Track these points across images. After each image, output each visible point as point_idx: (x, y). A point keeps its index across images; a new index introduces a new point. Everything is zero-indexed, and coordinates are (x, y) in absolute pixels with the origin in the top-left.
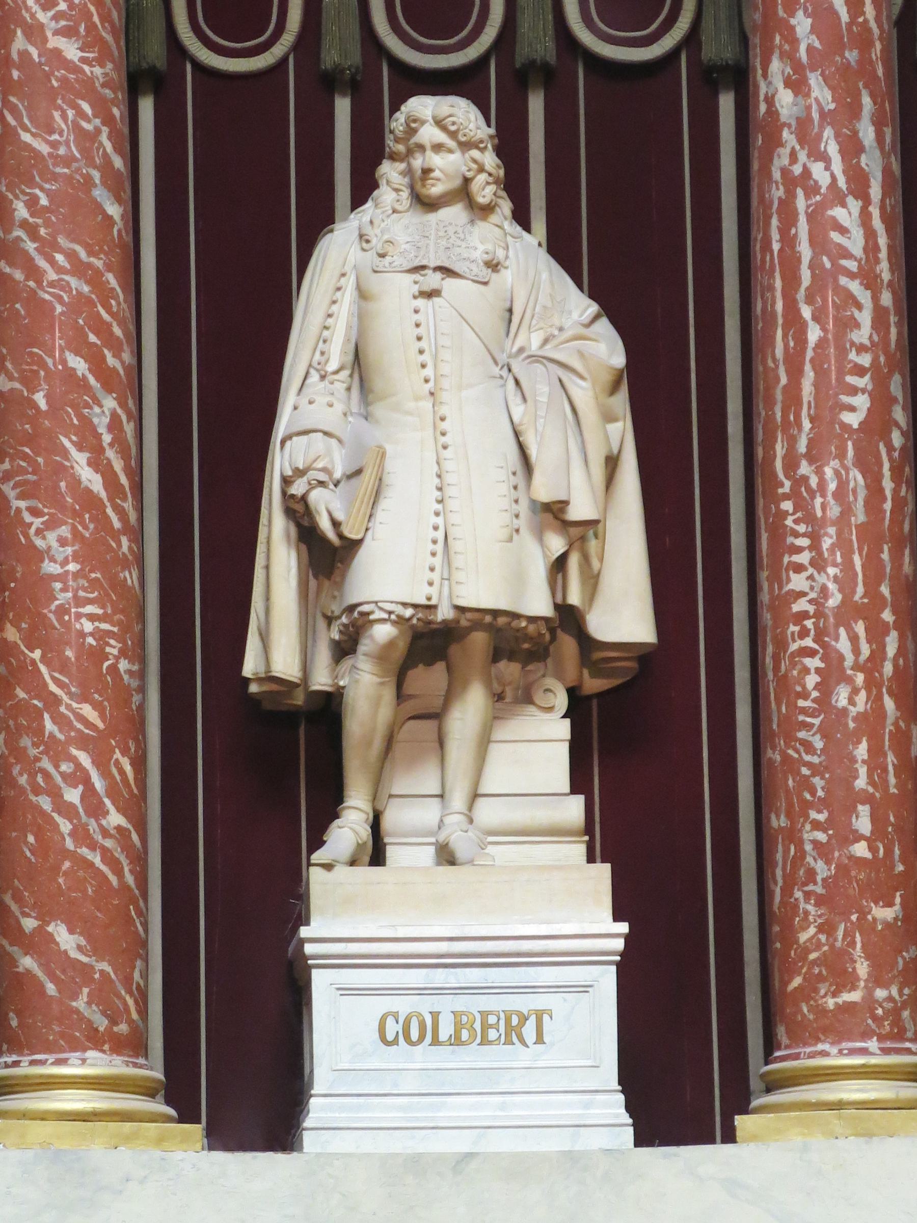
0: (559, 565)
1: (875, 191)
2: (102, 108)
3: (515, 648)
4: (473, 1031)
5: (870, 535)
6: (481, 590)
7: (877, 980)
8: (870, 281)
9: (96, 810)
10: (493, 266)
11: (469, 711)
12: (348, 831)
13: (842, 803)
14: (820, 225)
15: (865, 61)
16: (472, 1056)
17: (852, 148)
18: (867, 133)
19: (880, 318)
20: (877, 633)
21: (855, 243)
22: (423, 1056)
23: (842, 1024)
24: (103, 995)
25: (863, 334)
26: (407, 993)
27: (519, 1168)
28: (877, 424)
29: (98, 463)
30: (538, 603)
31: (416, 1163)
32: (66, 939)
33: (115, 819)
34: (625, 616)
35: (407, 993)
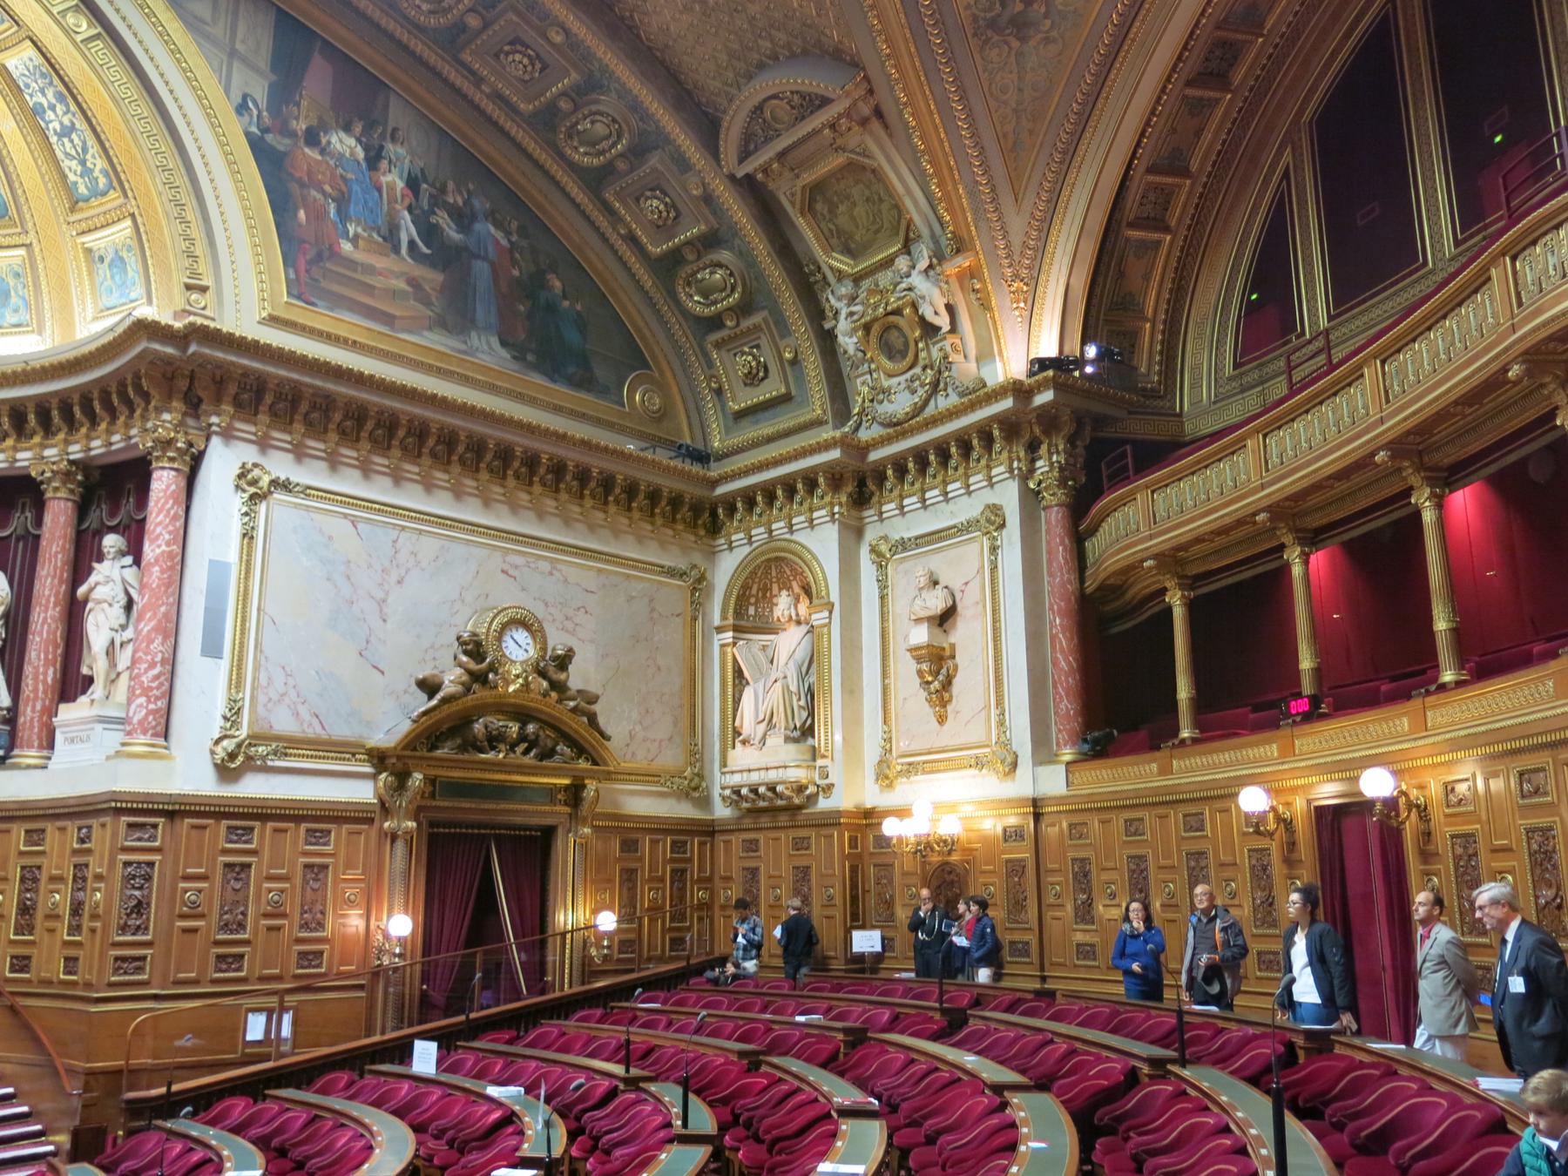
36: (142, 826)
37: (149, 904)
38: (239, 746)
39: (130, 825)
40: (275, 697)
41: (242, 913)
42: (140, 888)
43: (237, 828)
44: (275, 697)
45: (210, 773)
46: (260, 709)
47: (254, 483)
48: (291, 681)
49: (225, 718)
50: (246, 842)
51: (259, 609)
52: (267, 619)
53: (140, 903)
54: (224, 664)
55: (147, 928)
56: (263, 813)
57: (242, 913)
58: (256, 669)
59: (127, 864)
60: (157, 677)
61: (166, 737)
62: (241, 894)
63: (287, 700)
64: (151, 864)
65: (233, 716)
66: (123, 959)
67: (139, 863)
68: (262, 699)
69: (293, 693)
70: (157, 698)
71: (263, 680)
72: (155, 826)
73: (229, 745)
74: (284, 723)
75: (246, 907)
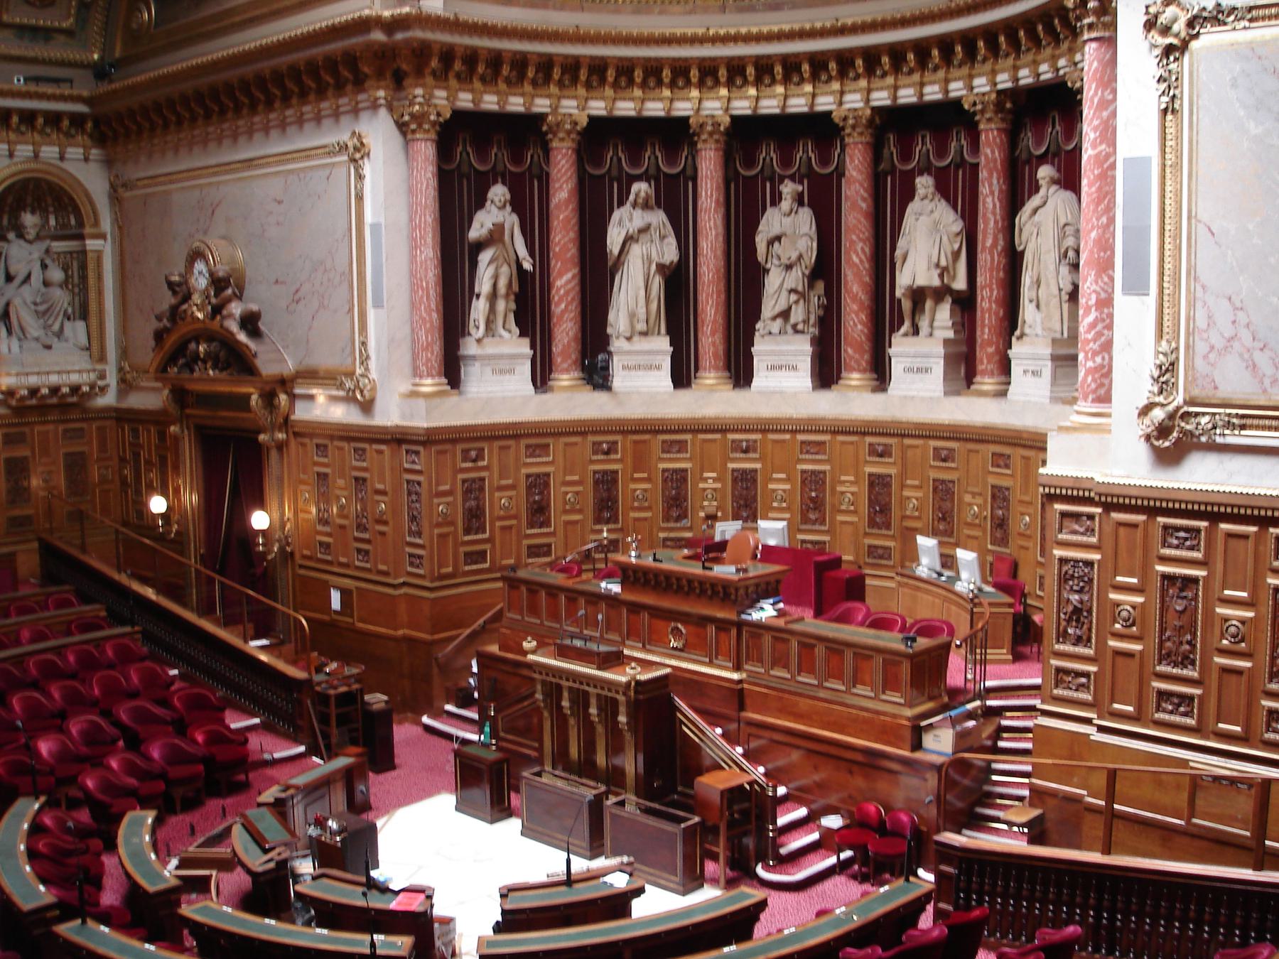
0: (941, 276)
1: (996, 194)
2: (861, 185)
3: (940, 293)
4: (919, 370)
5: (991, 270)
6: (921, 281)
7: (989, 362)
8: (994, 213)
9: (855, 325)
10: (932, 212)
11: (929, 304)
12: (906, 326)
13: (983, 326)
14: (984, 203)
15: (995, 166)
16: (920, 375)
17: (991, 185)
18: (995, 181)
19: (996, 222)
20: (991, 290)
21: (991, 206)
22: (911, 375)
23: (984, 373)
24: (857, 361)
25: (992, 224)
26: (908, 362)
27: (923, 399)
28: (995, 244)
29: (858, 255)
30: (936, 282)
31: (905, 397)
32: (850, 351)
33: (859, 327)
34: (960, 284)
35: (908, 362)
36: (1076, 516)
37: (1090, 611)
38: (1171, 416)
39: (1064, 515)
40: (1218, 342)
41: (1189, 643)
42: (1080, 591)
43: (1178, 529)
44: (1218, 342)
45: (1142, 450)
46: (1199, 362)
47: (1166, 31)
48: (1241, 316)
49: (1156, 380)
50: (1191, 548)
51: (1189, 218)
52: (1202, 230)
53: (1077, 611)
54: (1151, 300)
55: (1089, 640)
56: (1213, 511)
57: (1189, 643)
58: (1192, 305)
59: (1063, 561)
60: (1093, 325)
61: (1106, 398)
62: (1185, 618)
63: (1236, 344)
64: (1089, 564)
65: (1166, 373)
66: (1067, 672)
67: (1077, 561)
68: (1201, 347)
69: (1245, 335)
70: (1095, 354)
71: (1201, 322)
72: (1091, 517)
73: (1158, 414)
74: (1234, 381)
75: (1194, 635)
